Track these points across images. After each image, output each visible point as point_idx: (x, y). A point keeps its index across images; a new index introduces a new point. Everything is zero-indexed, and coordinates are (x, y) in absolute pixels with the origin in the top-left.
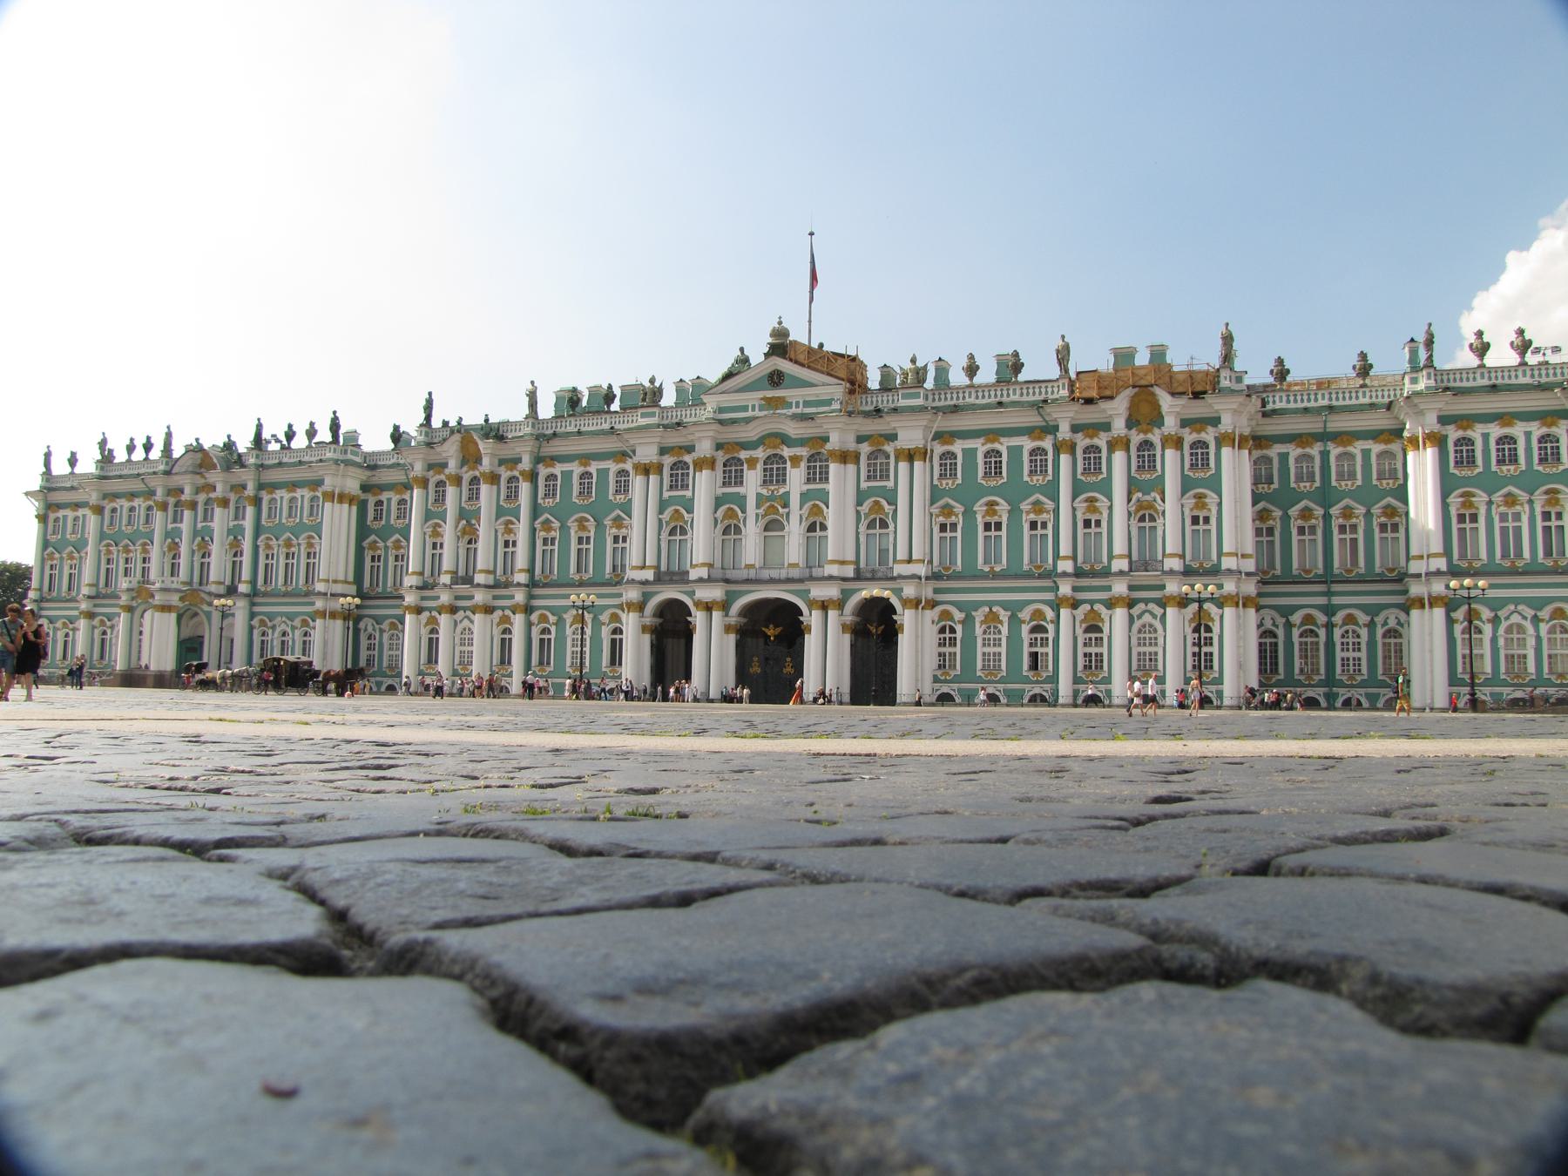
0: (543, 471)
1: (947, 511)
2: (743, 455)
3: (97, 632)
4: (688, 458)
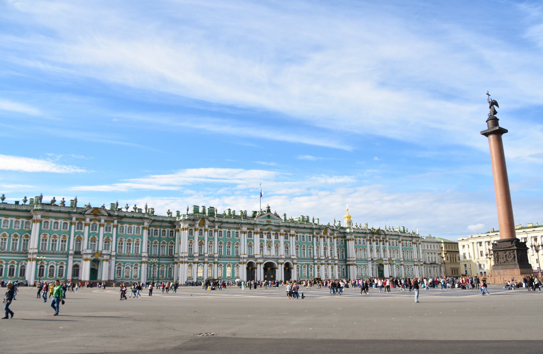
0: (219, 230)
1: (297, 246)
2: (264, 232)
3: (39, 266)
4: (252, 231)
